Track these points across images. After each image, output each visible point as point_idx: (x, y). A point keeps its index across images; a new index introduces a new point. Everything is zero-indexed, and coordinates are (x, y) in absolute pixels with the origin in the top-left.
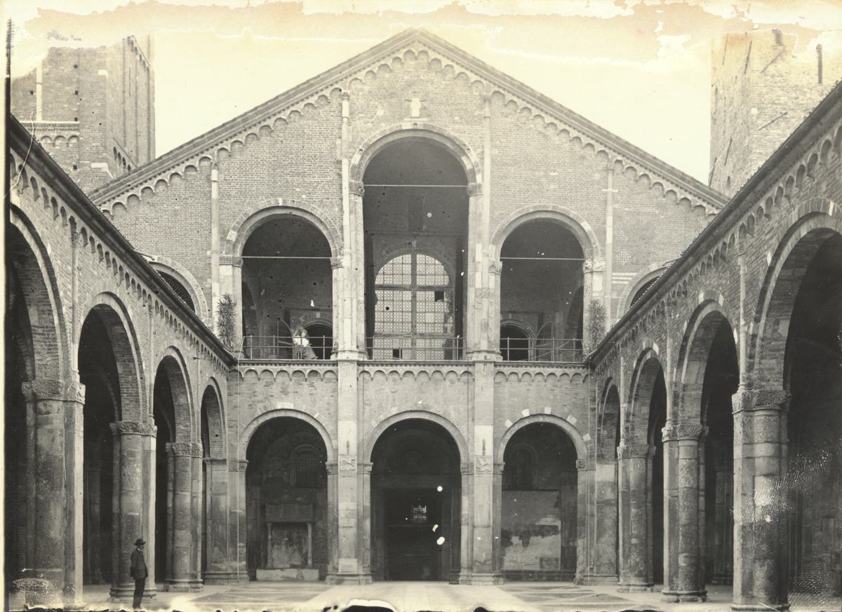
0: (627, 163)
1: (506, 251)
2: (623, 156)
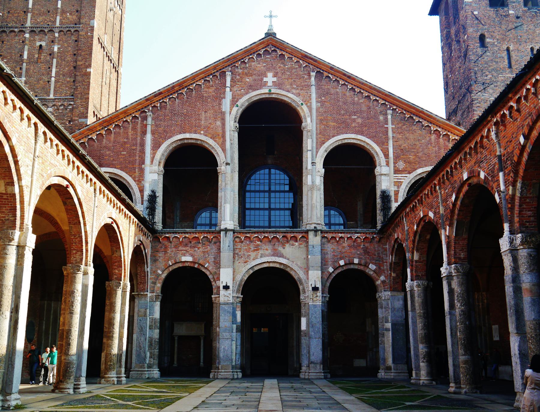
0: (399, 111)
1: (327, 163)
2: (397, 106)
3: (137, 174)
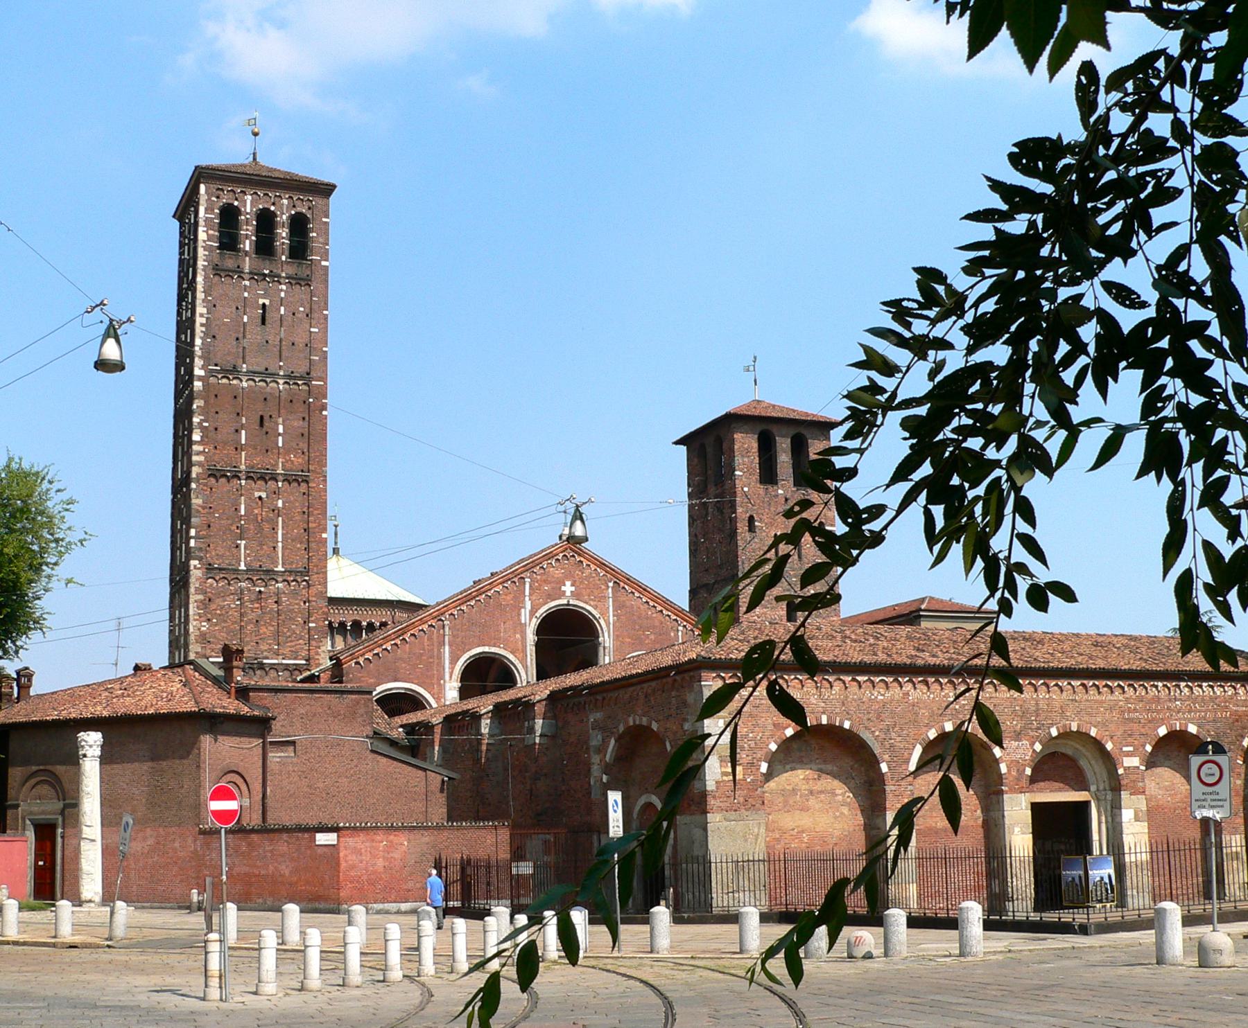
3: (436, 690)
